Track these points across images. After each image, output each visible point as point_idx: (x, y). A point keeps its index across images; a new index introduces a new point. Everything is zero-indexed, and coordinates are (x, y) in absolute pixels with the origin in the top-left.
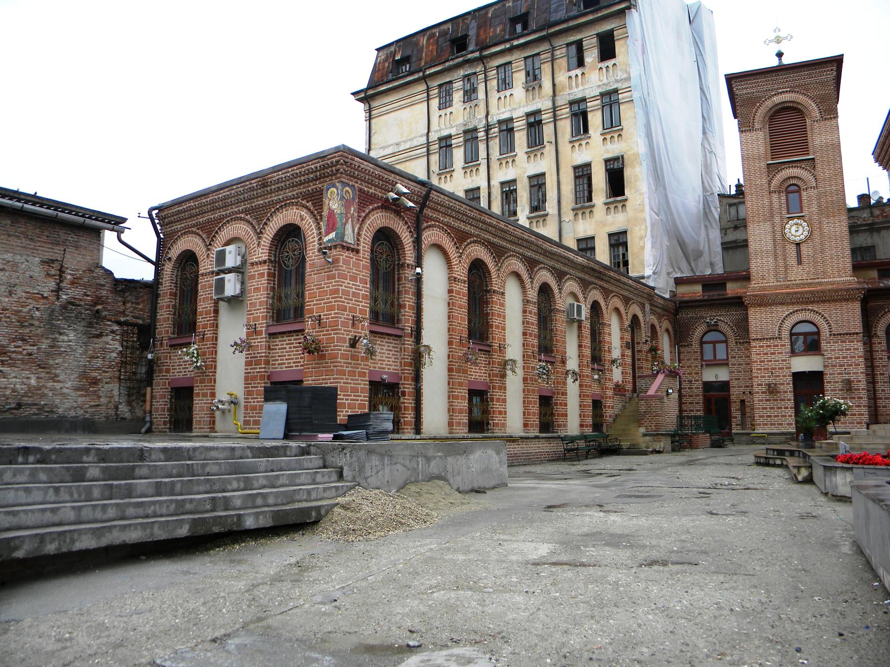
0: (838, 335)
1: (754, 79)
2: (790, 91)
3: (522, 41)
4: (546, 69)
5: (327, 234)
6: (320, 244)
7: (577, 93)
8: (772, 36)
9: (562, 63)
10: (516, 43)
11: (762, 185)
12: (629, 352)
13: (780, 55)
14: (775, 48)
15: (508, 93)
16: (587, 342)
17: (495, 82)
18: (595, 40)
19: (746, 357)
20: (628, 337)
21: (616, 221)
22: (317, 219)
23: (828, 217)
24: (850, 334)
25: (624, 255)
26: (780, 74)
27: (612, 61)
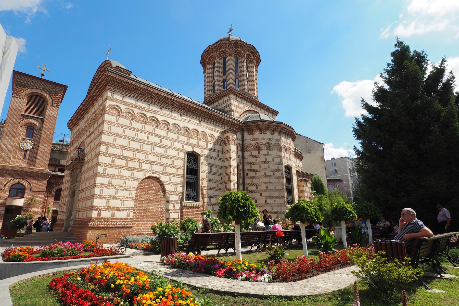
0: (34, 191)
1: (27, 78)
2: (42, 90)
11: (16, 122)
23: (43, 143)
24: (40, 192)
26: (40, 81)
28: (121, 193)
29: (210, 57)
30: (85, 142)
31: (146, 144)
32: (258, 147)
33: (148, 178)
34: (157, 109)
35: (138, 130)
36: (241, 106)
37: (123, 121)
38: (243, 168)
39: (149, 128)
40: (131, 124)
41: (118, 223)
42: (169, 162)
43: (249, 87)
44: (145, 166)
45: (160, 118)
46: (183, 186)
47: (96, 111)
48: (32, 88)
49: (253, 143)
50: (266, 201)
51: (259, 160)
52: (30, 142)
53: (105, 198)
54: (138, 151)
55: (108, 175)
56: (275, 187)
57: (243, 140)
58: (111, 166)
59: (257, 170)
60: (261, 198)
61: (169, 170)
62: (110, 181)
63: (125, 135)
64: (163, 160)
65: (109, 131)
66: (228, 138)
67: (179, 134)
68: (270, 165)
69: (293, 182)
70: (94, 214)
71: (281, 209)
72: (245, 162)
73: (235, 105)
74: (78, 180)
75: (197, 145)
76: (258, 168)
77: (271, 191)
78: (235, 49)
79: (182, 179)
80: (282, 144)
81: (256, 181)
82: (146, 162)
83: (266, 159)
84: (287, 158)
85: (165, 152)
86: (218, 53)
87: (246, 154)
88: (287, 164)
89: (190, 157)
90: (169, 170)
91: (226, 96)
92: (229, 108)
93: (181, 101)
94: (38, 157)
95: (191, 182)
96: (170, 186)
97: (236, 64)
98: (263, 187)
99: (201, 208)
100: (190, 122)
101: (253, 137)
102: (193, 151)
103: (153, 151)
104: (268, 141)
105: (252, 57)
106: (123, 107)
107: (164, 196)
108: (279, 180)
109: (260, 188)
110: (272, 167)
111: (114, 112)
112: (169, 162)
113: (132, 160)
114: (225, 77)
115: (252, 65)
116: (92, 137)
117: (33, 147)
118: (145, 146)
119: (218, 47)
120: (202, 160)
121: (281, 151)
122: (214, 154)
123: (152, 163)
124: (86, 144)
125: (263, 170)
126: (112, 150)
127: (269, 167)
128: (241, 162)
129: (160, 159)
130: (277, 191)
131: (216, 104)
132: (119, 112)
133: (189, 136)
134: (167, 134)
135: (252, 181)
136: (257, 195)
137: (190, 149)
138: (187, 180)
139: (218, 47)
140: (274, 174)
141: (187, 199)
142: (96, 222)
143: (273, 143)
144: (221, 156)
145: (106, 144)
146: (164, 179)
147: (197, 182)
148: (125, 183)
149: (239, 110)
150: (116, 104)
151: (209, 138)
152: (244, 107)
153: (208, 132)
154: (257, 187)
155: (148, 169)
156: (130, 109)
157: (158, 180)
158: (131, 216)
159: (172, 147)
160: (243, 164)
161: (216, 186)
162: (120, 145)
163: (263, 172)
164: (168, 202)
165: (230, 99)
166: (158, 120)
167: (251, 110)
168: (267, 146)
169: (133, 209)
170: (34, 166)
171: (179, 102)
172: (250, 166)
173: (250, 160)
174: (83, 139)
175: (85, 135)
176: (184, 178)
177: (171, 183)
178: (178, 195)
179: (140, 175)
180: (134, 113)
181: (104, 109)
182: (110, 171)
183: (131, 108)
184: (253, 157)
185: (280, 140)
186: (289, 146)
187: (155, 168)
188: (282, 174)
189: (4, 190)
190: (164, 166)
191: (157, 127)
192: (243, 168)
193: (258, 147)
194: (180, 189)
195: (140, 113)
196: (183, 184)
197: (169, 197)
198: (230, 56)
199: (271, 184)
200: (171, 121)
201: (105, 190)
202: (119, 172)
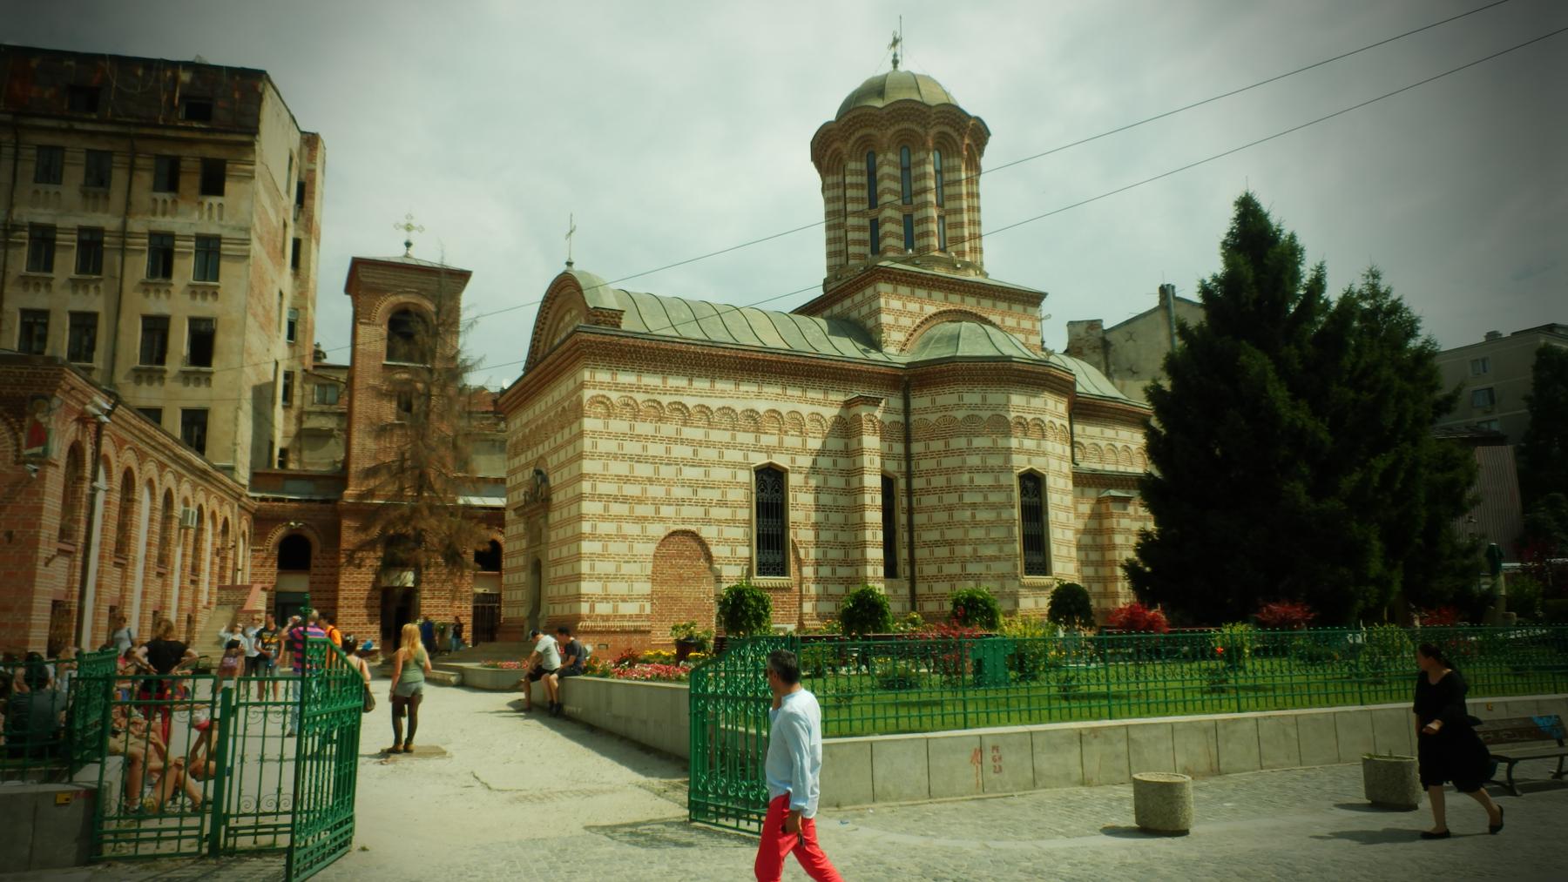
3: (89, 127)
4: (119, 177)
5: (30, 446)
6: (18, 456)
7: (163, 223)
8: (404, 222)
9: (145, 179)
10: (78, 126)
12: (217, 560)
13: (408, 244)
14: (404, 236)
15: (52, 188)
16: (190, 551)
17: (31, 167)
18: (197, 166)
20: (219, 542)
21: (195, 396)
22: (13, 429)
25: (198, 437)
27: (215, 200)
28: (626, 569)
29: (833, 152)
30: (549, 460)
31: (667, 464)
32: (948, 429)
33: (674, 533)
34: (681, 382)
35: (646, 438)
36: (913, 306)
37: (619, 425)
38: (909, 484)
39: (668, 429)
40: (632, 428)
41: (626, 624)
42: (715, 495)
44: (666, 511)
45: (691, 402)
46: (750, 545)
47: (563, 400)
48: (397, 294)
49: (933, 418)
50: (964, 568)
51: (948, 462)
53: (599, 578)
54: (650, 480)
55: (600, 535)
57: (907, 411)
58: (603, 518)
60: (951, 560)
61: (716, 513)
62: (605, 548)
64: (703, 494)
66: (857, 418)
69: (1047, 513)
70: (584, 608)
72: (913, 468)
73: (890, 311)
74: (543, 541)
75: (780, 448)
77: (978, 542)
78: (897, 127)
79: (747, 529)
80: (1013, 415)
81: (941, 517)
82: (669, 502)
83: (964, 461)
86: (851, 142)
87: (917, 448)
88: (1028, 467)
89: (765, 478)
91: (869, 284)
92: (876, 320)
93: (733, 353)
97: (906, 170)
99: (796, 588)
100: (758, 395)
101: (933, 401)
102: (771, 463)
103: (679, 477)
105: (955, 135)
106: (614, 396)
107: (711, 568)
108: (999, 515)
109: (951, 534)
110: (981, 480)
111: (599, 410)
112: (715, 495)
113: (640, 501)
114: (873, 213)
115: (957, 161)
116: (562, 455)
118: (663, 469)
119: (851, 126)
120: (794, 480)
122: (825, 462)
123: (680, 502)
124: (550, 466)
125: (956, 489)
126: (603, 488)
127: (972, 480)
128: (904, 468)
129: (695, 492)
130: (994, 541)
131: (847, 303)
133: (758, 430)
134: (707, 435)
135: (930, 518)
136: (942, 552)
137: (761, 460)
138: (758, 530)
140: (985, 497)
141: (761, 572)
142: (589, 623)
143: (986, 414)
145: (592, 477)
146: (707, 533)
147: (783, 531)
148: (631, 548)
150: (602, 392)
151: (808, 425)
153: (806, 410)
154: (942, 534)
155: (673, 515)
157: (694, 536)
158: (648, 610)
160: (909, 476)
165: (877, 296)
166: (687, 408)
167: (945, 312)
168: (972, 426)
169: (650, 598)
171: (730, 357)
173: (926, 465)
174: (541, 450)
176: (751, 527)
178: (739, 565)
179: (659, 531)
180: (637, 405)
181: (580, 404)
182: (606, 528)
183: (629, 395)
185: (1006, 406)
187: (687, 512)
188: (1010, 497)
191: (685, 424)
192: (909, 484)
194: (744, 552)
195: (649, 400)
196: (750, 540)
199: (976, 524)
200: (715, 404)
201: (598, 565)
202: (619, 528)
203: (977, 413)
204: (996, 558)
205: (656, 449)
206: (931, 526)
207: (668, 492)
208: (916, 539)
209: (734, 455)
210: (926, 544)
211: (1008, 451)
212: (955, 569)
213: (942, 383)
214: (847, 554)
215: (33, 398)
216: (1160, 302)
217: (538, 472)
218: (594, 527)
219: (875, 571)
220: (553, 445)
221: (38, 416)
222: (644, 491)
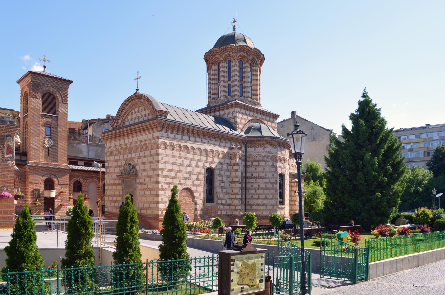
19: (23, 188)
30: (136, 161)
38: (246, 175)
39: (183, 154)
43: (252, 91)
45: (189, 145)
46: (204, 193)
49: (254, 154)
50: (262, 202)
51: (258, 169)
52: (50, 140)
53: (164, 203)
56: (270, 191)
59: (256, 178)
60: (258, 199)
63: (170, 161)
64: (193, 176)
65: (162, 160)
66: (235, 154)
67: (201, 155)
68: (267, 174)
69: (285, 186)
71: (273, 207)
72: (247, 170)
73: (240, 118)
76: (257, 176)
77: (266, 194)
81: (256, 186)
82: (183, 178)
83: (264, 169)
84: (281, 168)
85: (193, 170)
87: (249, 164)
88: (281, 172)
90: (197, 182)
92: (235, 120)
94: (59, 154)
95: (209, 190)
96: (197, 193)
98: (261, 191)
101: (255, 149)
102: (211, 167)
104: (266, 154)
108: (273, 186)
109: (258, 191)
117: (53, 144)
121: (277, 162)
123: (186, 179)
124: (136, 162)
125: (261, 178)
126: (165, 173)
127: (266, 175)
128: (244, 170)
129: (190, 175)
130: (271, 194)
131: (222, 112)
132: (165, 146)
134: (193, 157)
135: (252, 186)
136: (256, 197)
137: (208, 166)
139: (224, 51)
140: (270, 180)
143: (271, 155)
144: (229, 167)
145: (161, 169)
146: (193, 189)
149: (243, 121)
152: (247, 118)
154: (256, 191)
156: (171, 142)
159: (197, 166)
160: (246, 172)
161: (226, 192)
162: (168, 169)
163: (261, 179)
164: (196, 204)
166: (188, 147)
170: (57, 162)
172: (251, 174)
175: (133, 155)
177: (198, 192)
180: (174, 145)
183: (172, 142)
184: (254, 166)
185: (276, 153)
186: (284, 156)
188: (276, 181)
189: (40, 183)
190: (193, 180)
192: (246, 175)
193: (258, 159)
195: (177, 144)
197: (197, 201)
198: (235, 61)
199: (266, 189)
203: (268, 154)
204: (272, 199)
205: (179, 161)
206: (252, 188)
207: (183, 175)
208: (247, 192)
209: (200, 164)
210: (250, 194)
211: (276, 167)
212: (260, 202)
213: (254, 144)
214: (229, 196)
215: (7, 136)
216: (292, 116)
217: (130, 164)
218: (162, 186)
219: (239, 202)
220: (138, 154)
221: (9, 143)
222: (176, 174)
